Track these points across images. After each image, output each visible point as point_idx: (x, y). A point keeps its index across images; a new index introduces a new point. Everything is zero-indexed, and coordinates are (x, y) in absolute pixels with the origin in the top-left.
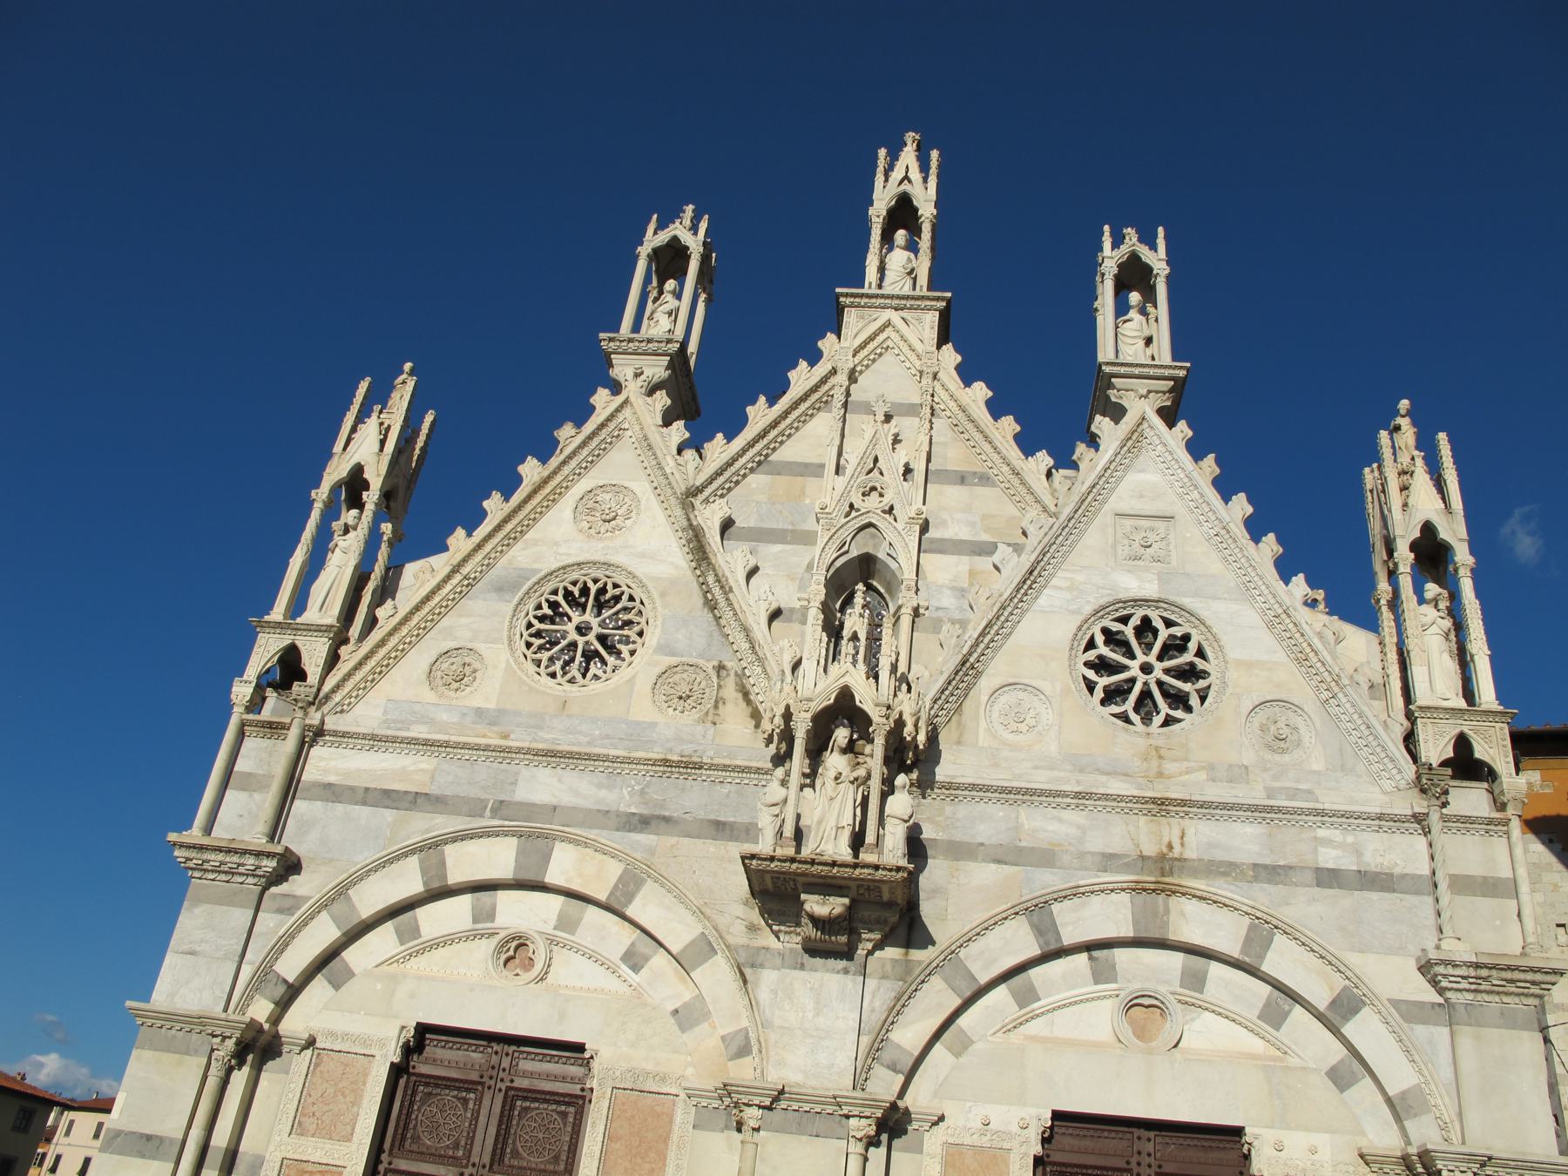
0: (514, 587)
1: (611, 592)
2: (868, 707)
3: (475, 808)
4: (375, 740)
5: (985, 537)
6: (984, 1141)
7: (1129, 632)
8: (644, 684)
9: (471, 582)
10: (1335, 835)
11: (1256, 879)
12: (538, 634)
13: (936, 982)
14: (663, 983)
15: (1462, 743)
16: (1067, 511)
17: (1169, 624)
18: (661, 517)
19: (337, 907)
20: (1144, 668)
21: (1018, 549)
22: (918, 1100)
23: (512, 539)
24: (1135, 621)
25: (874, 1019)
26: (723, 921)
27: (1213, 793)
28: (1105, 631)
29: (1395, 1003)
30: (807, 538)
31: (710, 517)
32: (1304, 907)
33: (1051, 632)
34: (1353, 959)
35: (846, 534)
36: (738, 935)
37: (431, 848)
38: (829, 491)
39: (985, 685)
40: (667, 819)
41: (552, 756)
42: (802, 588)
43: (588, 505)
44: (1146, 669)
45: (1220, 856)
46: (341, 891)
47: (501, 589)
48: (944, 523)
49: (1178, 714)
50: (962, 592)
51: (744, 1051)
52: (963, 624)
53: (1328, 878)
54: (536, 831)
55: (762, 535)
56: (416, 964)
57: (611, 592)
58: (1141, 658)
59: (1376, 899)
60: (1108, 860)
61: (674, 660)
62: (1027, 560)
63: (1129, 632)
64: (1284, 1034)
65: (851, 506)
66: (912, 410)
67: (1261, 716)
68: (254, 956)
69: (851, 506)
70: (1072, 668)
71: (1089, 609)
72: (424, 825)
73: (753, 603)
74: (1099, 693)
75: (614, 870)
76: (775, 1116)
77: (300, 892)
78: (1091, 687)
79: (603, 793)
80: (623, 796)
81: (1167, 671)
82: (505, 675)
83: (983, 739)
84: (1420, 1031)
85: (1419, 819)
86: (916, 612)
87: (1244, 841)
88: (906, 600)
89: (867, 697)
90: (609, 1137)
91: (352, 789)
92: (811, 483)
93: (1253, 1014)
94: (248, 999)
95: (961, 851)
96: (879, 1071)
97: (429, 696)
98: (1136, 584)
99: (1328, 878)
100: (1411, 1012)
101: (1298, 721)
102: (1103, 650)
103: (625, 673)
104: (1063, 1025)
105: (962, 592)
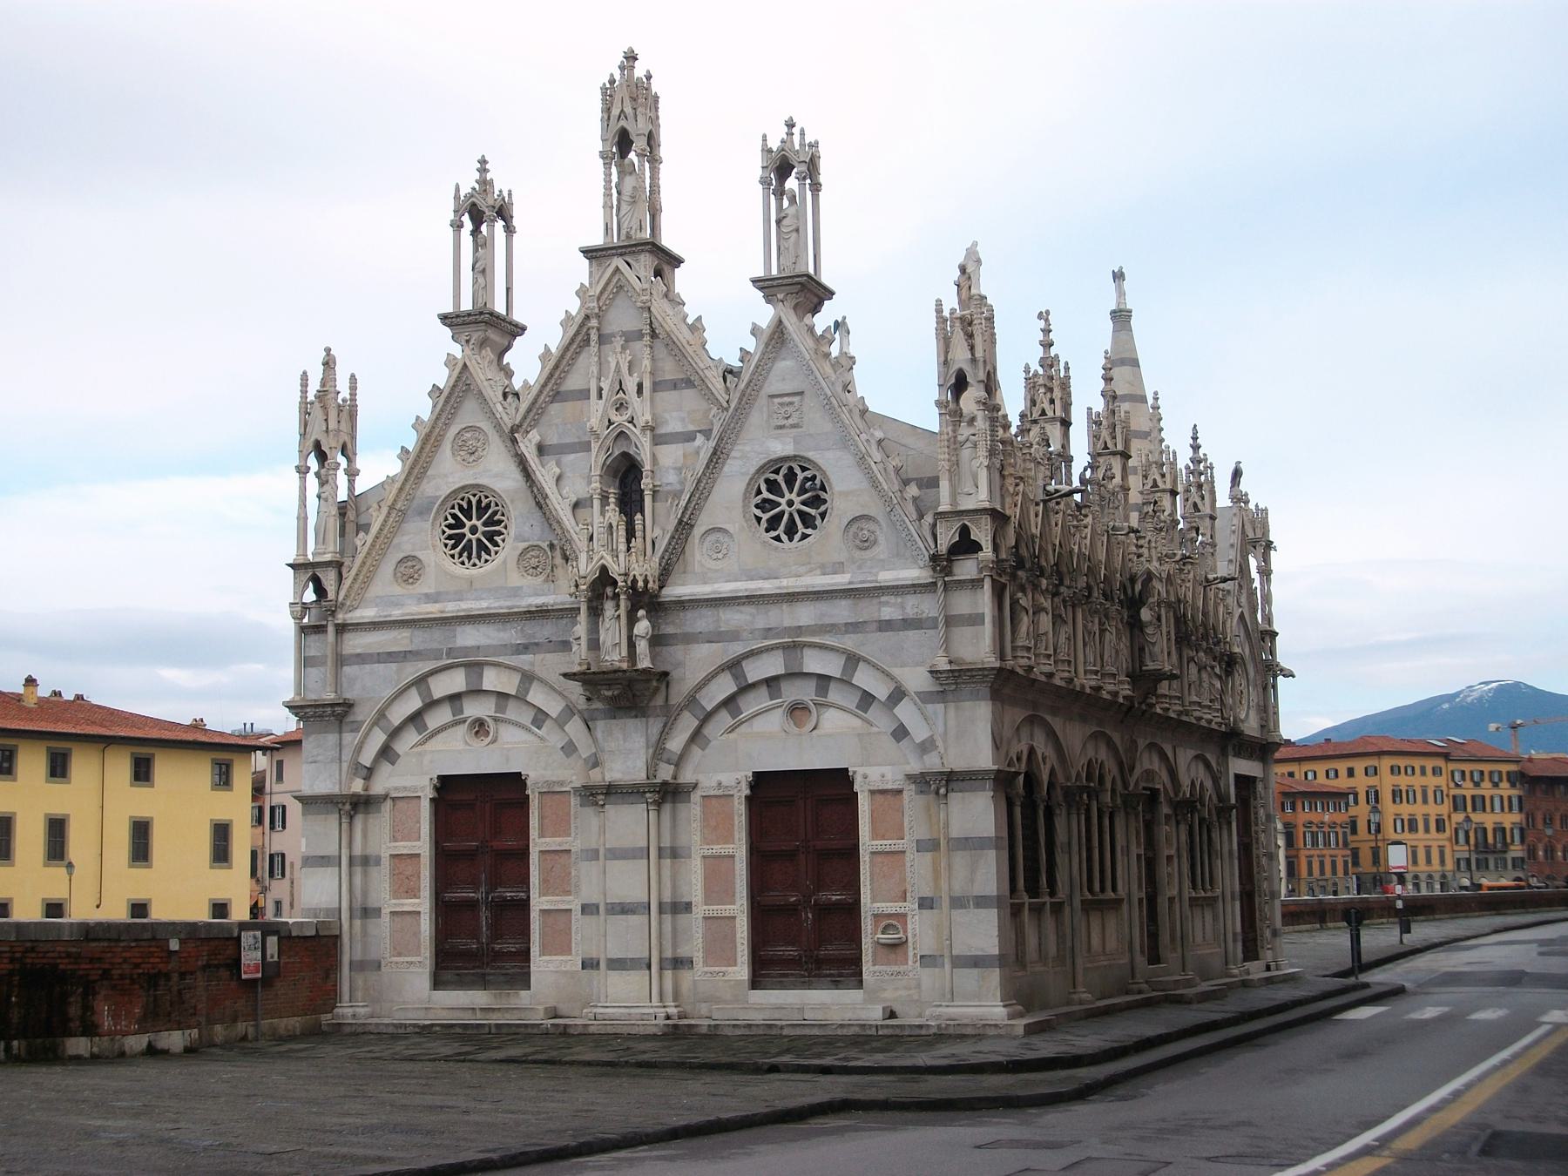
0: (429, 510)
1: (485, 502)
2: (615, 576)
4: (375, 626)
5: (691, 428)
6: (720, 793)
7: (780, 478)
8: (512, 564)
9: (403, 513)
10: (892, 599)
11: (847, 632)
12: (450, 537)
13: (686, 715)
15: (965, 531)
16: (733, 406)
17: (804, 469)
18: (503, 448)
19: (383, 722)
20: (791, 501)
21: (707, 433)
22: (687, 777)
23: (420, 478)
24: (783, 471)
25: (654, 739)
26: (573, 698)
28: (767, 481)
29: (918, 694)
30: (586, 447)
32: (870, 645)
34: (896, 672)
35: (609, 442)
36: (581, 703)
37: (421, 682)
38: (596, 413)
39: (697, 532)
40: (537, 644)
44: (790, 503)
45: (827, 621)
46: (381, 715)
47: (421, 513)
48: (666, 422)
49: (808, 531)
50: (679, 470)
51: (596, 764)
53: (885, 626)
55: (563, 449)
56: (429, 746)
57: (485, 502)
58: (788, 496)
59: (912, 635)
61: (526, 544)
62: (712, 444)
63: (780, 478)
64: (870, 715)
65: (610, 423)
66: (639, 335)
67: (854, 528)
68: (347, 755)
69: (610, 423)
70: (745, 513)
71: (753, 470)
74: (764, 524)
76: (612, 798)
77: (359, 718)
78: (759, 519)
79: (502, 634)
81: (803, 503)
83: (697, 568)
84: (930, 706)
85: (930, 587)
86: (655, 493)
87: (841, 612)
88: (646, 483)
89: (615, 570)
90: (542, 818)
91: (371, 655)
93: (853, 706)
94: (352, 780)
95: (690, 639)
96: (663, 765)
97: (398, 590)
98: (781, 447)
99: (885, 626)
100: (926, 697)
101: (872, 526)
102: (766, 494)
103: (501, 556)
104: (759, 725)
105: (679, 470)
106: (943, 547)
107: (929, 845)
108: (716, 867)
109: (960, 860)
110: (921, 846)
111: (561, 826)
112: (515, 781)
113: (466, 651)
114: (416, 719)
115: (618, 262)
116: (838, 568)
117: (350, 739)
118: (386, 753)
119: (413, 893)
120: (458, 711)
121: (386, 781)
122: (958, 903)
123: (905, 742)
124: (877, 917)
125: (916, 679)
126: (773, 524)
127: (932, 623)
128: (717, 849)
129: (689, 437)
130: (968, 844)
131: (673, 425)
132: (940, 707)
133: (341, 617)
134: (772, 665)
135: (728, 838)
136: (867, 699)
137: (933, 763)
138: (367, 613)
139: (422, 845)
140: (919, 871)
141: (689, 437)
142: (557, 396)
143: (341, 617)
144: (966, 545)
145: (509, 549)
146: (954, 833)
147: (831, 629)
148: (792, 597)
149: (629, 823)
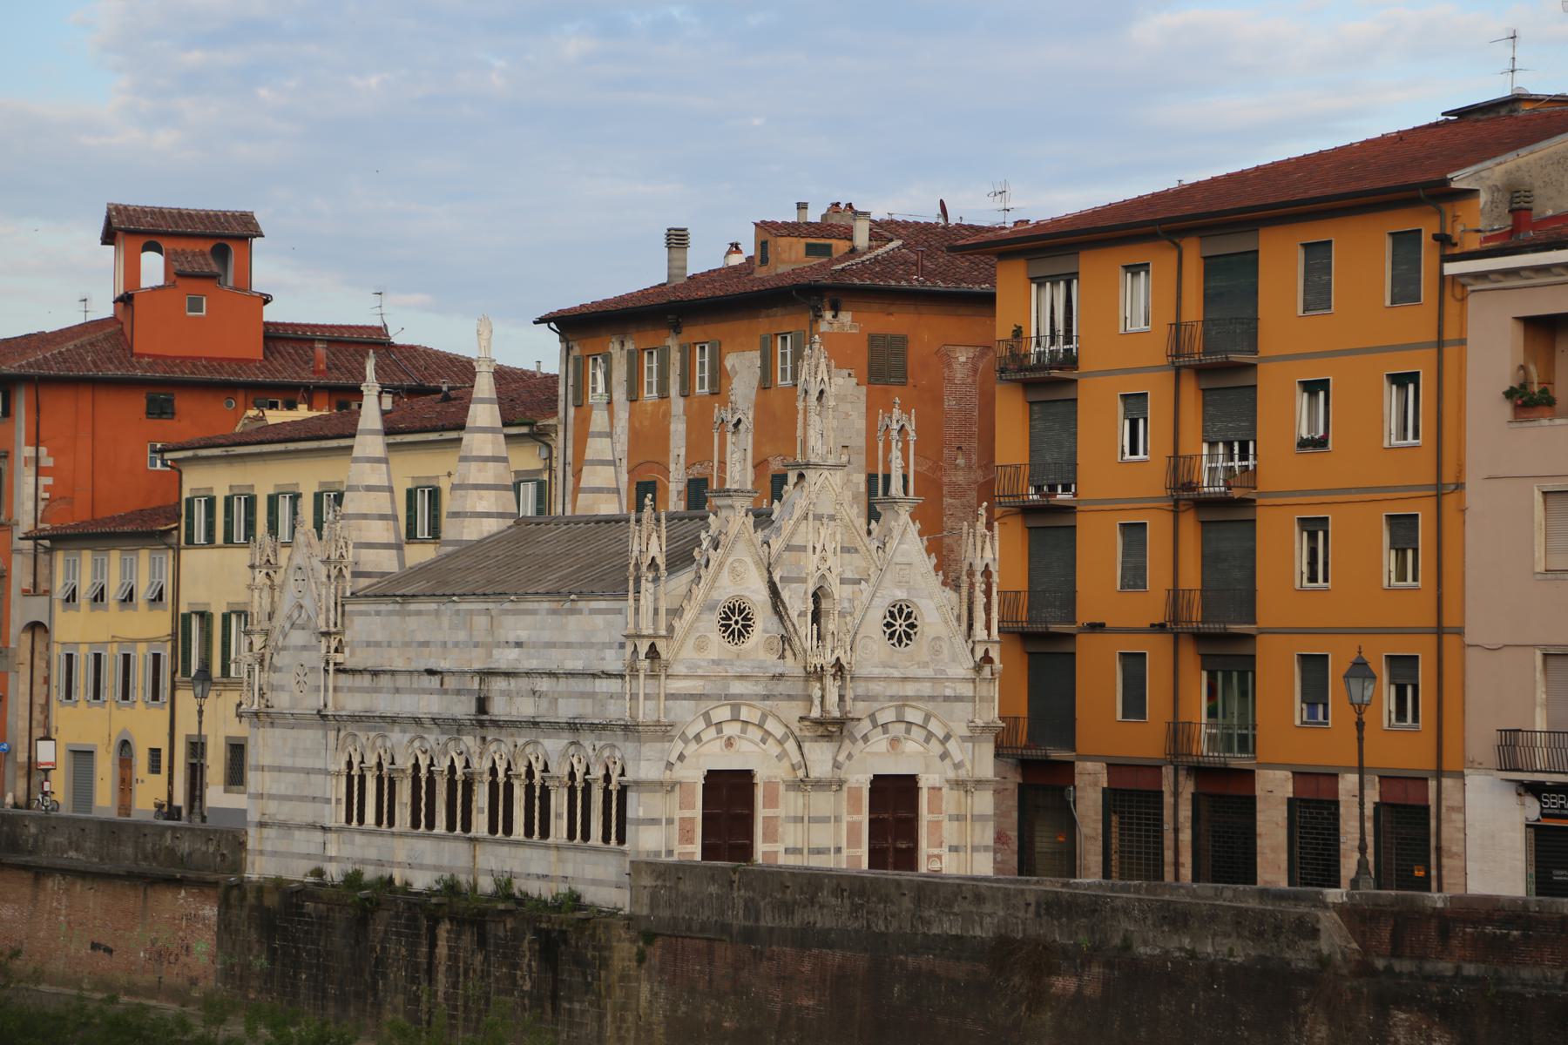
3: (719, 698)
14: (772, 748)
15: (987, 651)
27: (921, 673)
30: (804, 580)
31: (776, 579)
33: (877, 615)
39: (858, 637)
41: (742, 677)
42: (805, 601)
43: (733, 569)
50: (851, 601)
52: (851, 614)
54: (735, 702)
59: (959, 705)
60: (892, 698)
66: (832, 518)
72: (705, 705)
73: (794, 614)
75: (759, 714)
80: (759, 689)
82: (717, 644)
89: (844, 661)
92: (803, 554)
98: (900, 594)
99: (947, 699)
100: (964, 739)
106: (978, 657)
107: (958, 818)
108: (853, 829)
109: (978, 826)
110: (951, 818)
111: (772, 801)
112: (749, 774)
113: (734, 697)
114: (698, 738)
115: (826, 473)
116: (926, 665)
117: (667, 745)
118: (681, 757)
119: (691, 841)
120: (720, 731)
121: (682, 773)
122: (974, 849)
123: (948, 761)
124: (929, 857)
125: (961, 729)
126: (892, 636)
127: (973, 699)
128: (855, 817)
129: (858, 582)
130: (982, 818)
131: (848, 575)
132: (970, 745)
133: (670, 671)
134: (887, 716)
135: (859, 812)
136: (930, 735)
137: (963, 774)
138: (684, 671)
139: (697, 813)
140: (950, 832)
141: (858, 582)
142: (789, 548)
143: (670, 671)
144: (987, 659)
145: (757, 635)
146: (976, 812)
147: (919, 698)
148: (905, 679)
149: (822, 803)
